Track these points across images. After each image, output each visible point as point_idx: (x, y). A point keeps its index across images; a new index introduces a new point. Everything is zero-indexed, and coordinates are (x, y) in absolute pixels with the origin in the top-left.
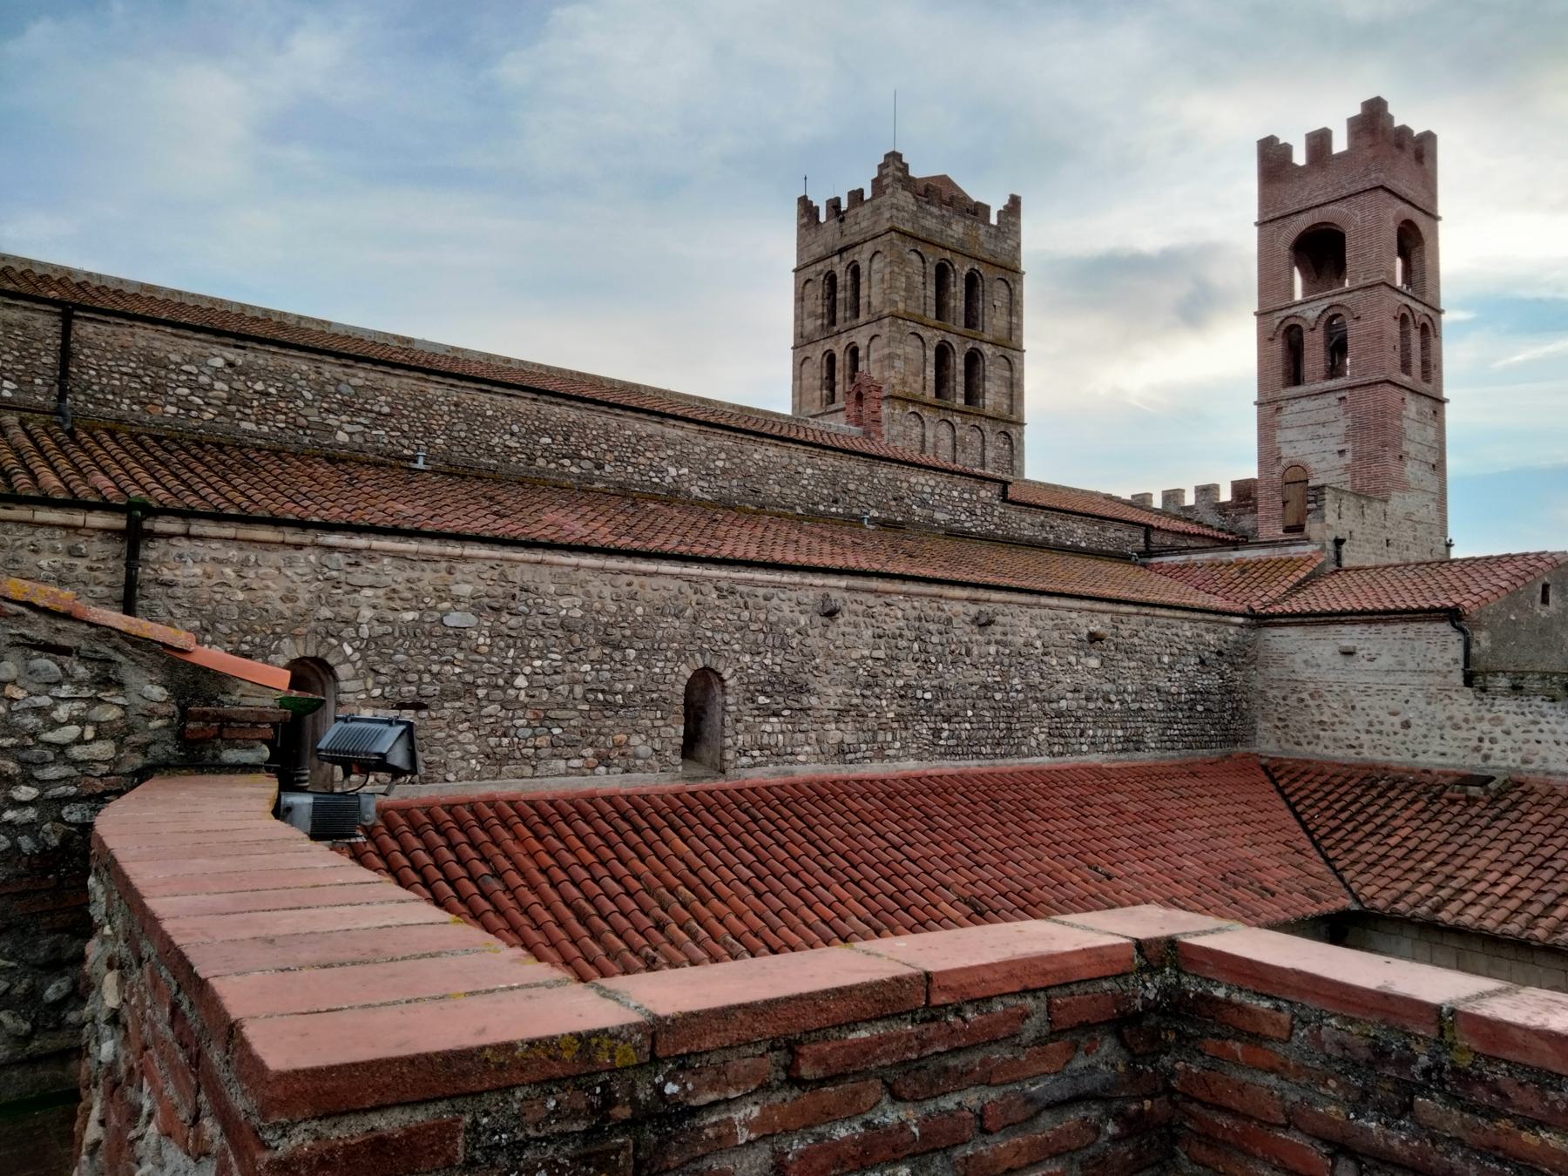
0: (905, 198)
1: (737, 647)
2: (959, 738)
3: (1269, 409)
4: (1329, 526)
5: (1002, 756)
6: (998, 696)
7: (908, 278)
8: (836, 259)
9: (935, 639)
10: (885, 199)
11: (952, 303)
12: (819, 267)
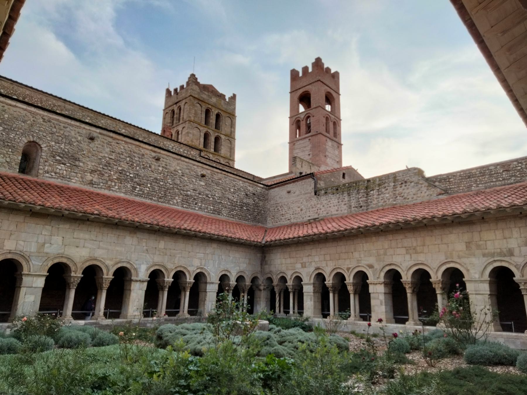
0: (195, 87)
1: (49, 139)
2: (143, 192)
3: (292, 144)
4: (298, 168)
5: (162, 202)
6: (162, 183)
7: (195, 111)
8: (175, 106)
9: (136, 159)
10: (190, 87)
11: (211, 121)
12: (170, 108)
